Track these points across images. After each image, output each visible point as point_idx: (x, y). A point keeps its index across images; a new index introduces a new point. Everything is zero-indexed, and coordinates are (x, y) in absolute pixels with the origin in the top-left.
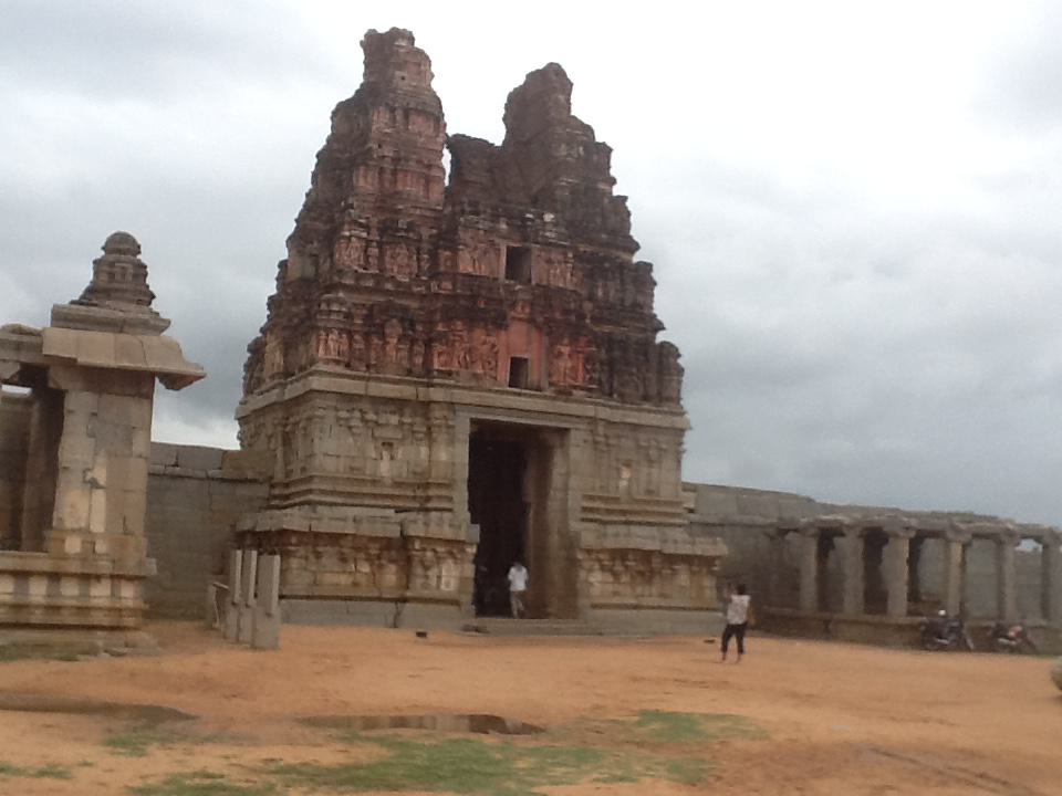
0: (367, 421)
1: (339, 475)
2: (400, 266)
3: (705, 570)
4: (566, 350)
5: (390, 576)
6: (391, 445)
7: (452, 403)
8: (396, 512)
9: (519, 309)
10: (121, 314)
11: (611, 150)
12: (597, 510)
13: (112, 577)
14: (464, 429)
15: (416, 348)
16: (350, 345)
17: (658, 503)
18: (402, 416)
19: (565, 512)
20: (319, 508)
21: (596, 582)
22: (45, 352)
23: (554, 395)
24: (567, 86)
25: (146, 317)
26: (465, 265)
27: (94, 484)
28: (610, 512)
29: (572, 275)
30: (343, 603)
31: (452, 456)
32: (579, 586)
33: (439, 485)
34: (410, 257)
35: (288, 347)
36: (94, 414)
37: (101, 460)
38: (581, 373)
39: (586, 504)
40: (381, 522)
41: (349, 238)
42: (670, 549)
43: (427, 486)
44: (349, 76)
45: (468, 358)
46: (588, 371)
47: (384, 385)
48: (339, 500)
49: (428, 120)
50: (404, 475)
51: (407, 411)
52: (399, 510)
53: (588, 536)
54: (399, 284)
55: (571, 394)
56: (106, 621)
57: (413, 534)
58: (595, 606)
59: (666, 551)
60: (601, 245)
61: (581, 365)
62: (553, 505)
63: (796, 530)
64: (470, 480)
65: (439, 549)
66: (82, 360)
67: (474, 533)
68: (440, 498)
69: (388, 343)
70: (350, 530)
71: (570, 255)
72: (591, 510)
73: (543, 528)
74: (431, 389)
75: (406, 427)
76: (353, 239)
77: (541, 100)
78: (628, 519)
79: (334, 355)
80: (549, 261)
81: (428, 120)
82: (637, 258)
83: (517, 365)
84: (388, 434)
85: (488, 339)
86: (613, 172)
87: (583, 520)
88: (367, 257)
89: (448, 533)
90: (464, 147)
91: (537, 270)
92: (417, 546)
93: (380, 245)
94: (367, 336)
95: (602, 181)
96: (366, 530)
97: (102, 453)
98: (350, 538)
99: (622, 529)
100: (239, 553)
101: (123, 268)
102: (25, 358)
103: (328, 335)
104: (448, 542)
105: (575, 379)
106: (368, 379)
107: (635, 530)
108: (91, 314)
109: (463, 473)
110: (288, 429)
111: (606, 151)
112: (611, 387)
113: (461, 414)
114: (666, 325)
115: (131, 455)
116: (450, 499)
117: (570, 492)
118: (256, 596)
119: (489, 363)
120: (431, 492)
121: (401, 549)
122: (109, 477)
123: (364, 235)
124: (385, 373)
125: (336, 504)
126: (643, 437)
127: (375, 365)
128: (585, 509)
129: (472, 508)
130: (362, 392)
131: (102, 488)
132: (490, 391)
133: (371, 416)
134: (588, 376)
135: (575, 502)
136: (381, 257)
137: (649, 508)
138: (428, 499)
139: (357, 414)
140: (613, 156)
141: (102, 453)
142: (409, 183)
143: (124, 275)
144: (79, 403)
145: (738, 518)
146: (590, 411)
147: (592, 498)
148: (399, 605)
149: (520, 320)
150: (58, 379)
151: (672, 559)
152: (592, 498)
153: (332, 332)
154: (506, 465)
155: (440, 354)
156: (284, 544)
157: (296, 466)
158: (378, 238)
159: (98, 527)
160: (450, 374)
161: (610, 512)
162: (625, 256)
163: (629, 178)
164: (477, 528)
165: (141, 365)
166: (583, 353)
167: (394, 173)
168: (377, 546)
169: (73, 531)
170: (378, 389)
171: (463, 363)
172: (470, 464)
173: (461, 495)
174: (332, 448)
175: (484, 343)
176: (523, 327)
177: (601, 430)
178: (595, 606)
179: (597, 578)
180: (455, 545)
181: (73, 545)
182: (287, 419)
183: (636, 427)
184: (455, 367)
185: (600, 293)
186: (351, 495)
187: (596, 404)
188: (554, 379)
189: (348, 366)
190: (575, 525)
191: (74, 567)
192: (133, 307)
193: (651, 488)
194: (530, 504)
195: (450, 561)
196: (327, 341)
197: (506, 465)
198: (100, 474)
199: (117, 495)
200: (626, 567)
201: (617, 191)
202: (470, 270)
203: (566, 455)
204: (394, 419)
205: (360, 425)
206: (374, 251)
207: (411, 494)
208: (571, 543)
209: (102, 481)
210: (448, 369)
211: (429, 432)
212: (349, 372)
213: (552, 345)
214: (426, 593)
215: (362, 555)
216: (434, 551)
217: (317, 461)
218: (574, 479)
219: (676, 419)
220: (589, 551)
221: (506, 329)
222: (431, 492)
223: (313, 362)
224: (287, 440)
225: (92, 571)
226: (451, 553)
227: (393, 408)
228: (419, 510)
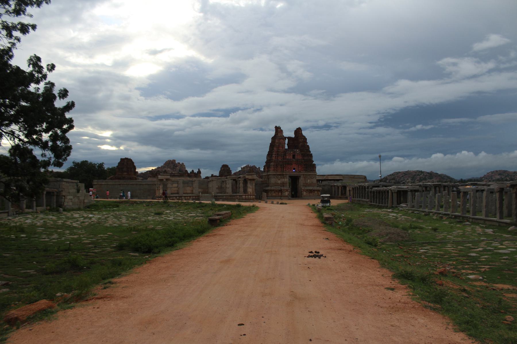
5: (280, 194)
14: (288, 177)
21: (305, 193)
26: (287, 157)
31: (287, 180)
35: (268, 168)
40: (278, 188)
44: (273, 133)
53: (303, 188)
77: (298, 131)
78: (309, 185)
90: (290, 138)
121: (281, 191)
144: (249, 182)
151: (314, 190)
154: (294, 180)
163: (309, 143)
173: (288, 184)
174: (273, 180)
179: (304, 193)
197: (294, 180)
199: (252, 189)
208: (301, 189)
218: (301, 181)
224: (268, 179)
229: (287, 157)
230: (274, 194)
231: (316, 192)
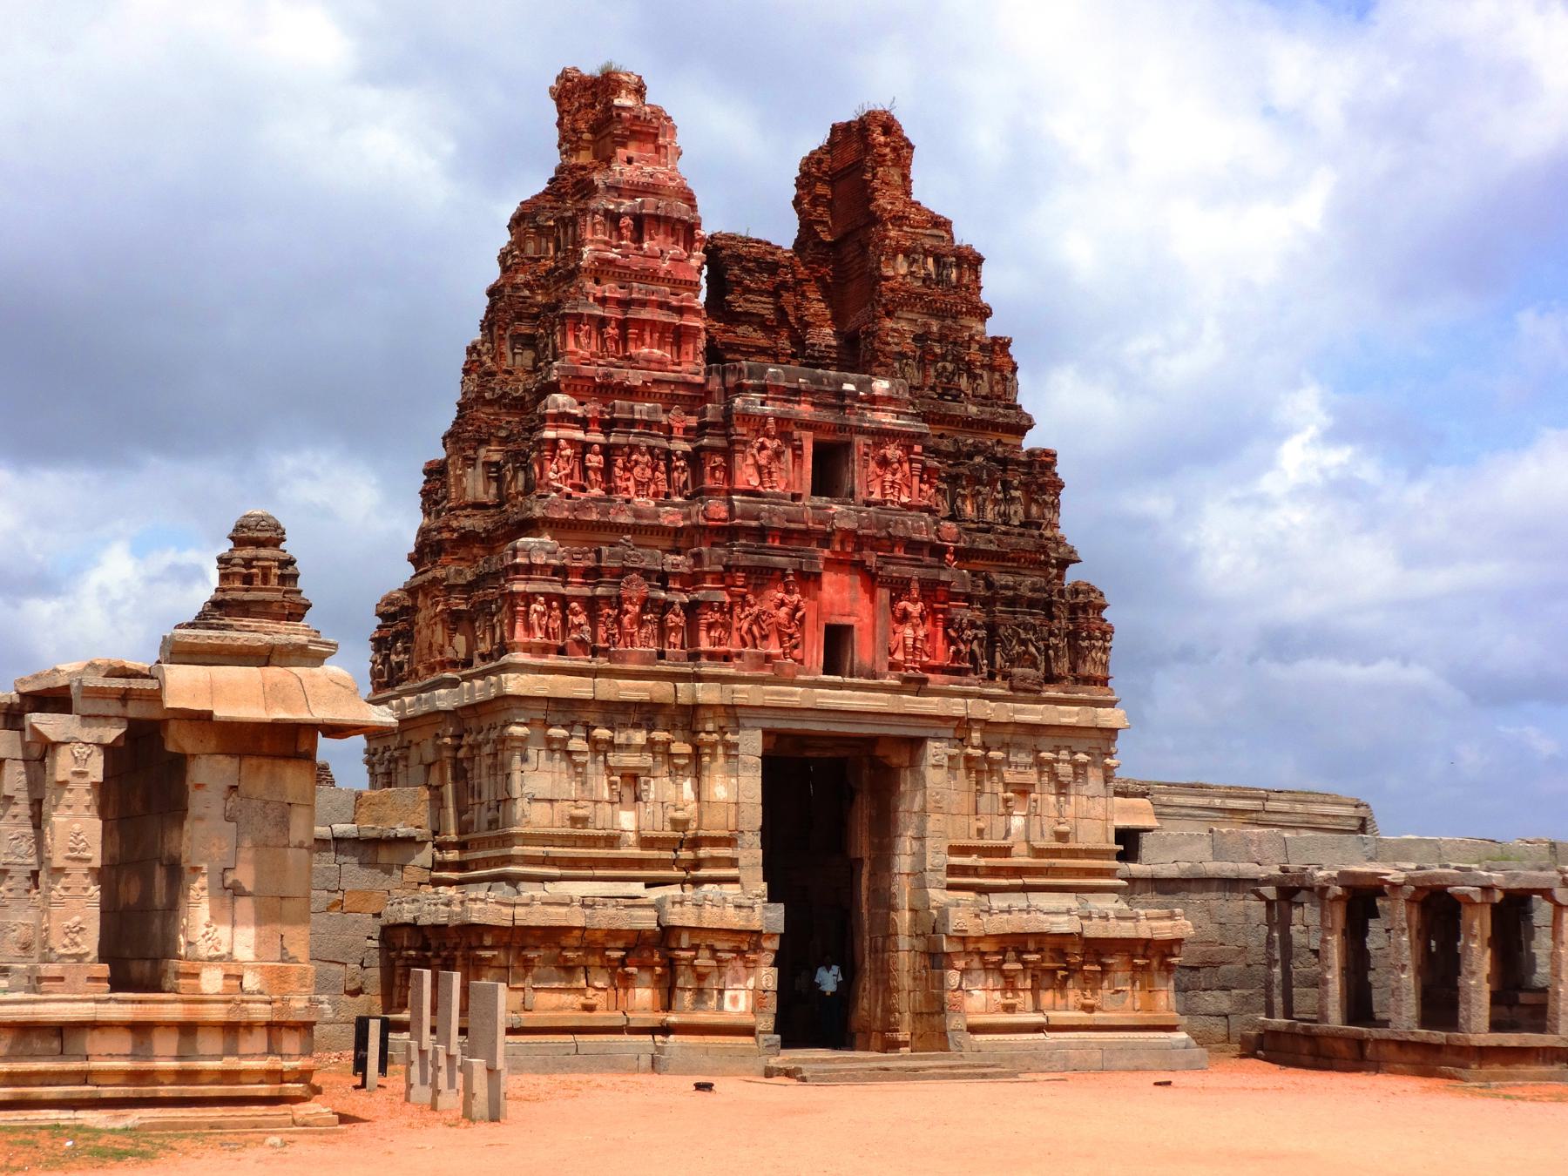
1: (554, 831)
2: (638, 483)
3: (1155, 963)
4: (915, 609)
5: (644, 994)
6: (635, 778)
7: (733, 706)
8: (647, 886)
10: (267, 638)
11: (979, 260)
12: (974, 871)
13: (269, 1025)
14: (751, 743)
15: (672, 619)
16: (565, 620)
17: (1074, 853)
18: (650, 730)
19: (918, 874)
20: (523, 886)
22: (169, 704)
23: (897, 683)
24: (902, 151)
25: (302, 639)
27: (237, 891)
28: (995, 872)
30: (570, 1038)
31: (733, 792)
32: (948, 995)
33: (715, 842)
34: (655, 469)
36: (234, 788)
37: (247, 854)
38: (940, 643)
39: (957, 860)
41: (555, 441)
42: (1094, 930)
43: (696, 843)
45: (755, 629)
46: (951, 641)
48: (556, 872)
50: (658, 825)
51: (660, 720)
52: (651, 884)
54: (638, 514)
55: (925, 680)
56: (264, 1090)
57: (678, 923)
58: (974, 1029)
59: (1088, 934)
60: (970, 424)
61: (940, 629)
62: (903, 863)
63: (1310, 889)
64: (762, 829)
65: (718, 945)
66: (221, 712)
67: (771, 918)
68: (716, 862)
69: (627, 612)
70: (577, 918)
71: (918, 449)
73: (885, 902)
74: (699, 685)
75: (659, 748)
76: (562, 442)
78: (1025, 880)
79: (539, 637)
80: (884, 463)
82: (1030, 441)
83: (837, 639)
84: (630, 760)
85: (787, 598)
86: (986, 297)
87: (951, 887)
88: (585, 470)
89: (735, 920)
91: (866, 480)
92: (685, 942)
93: (608, 451)
94: (591, 605)
96: (605, 918)
97: (247, 843)
98: (577, 933)
99: (1018, 900)
100: (427, 973)
101: (263, 568)
102: (134, 710)
103: (528, 606)
106: (595, 673)
107: (1038, 899)
108: (228, 642)
109: (754, 816)
110: (461, 754)
111: (971, 261)
112: (992, 663)
114: (1080, 555)
115: (287, 846)
116: (733, 863)
117: (929, 843)
118: (433, 1030)
119: (791, 636)
120: (704, 852)
122: (257, 881)
123: (579, 435)
124: (623, 661)
125: (552, 879)
127: (606, 649)
128: (953, 870)
129: (771, 872)
130: (590, 696)
131: (249, 895)
132: (793, 683)
133: (602, 733)
134: (953, 648)
135: (938, 858)
136: (607, 471)
138: (697, 864)
139: (580, 732)
140: (985, 270)
141: (247, 843)
142: (648, 340)
143: (265, 579)
144: (210, 775)
145: (1212, 867)
148: (658, 1038)
150: (178, 740)
151: (1098, 949)
153: (535, 601)
154: (827, 805)
155: (710, 627)
156: (471, 948)
157: (481, 816)
158: (601, 438)
159: (245, 953)
160: (727, 657)
161: (995, 872)
162: (1008, 439)
164: (778, 911)
165: (303, 715)
167: (623, 325)
168: (620, 944)
169: (211, 959)
170: (608, 689)
171: (748, 638)
172: (766, 803)
173: (751, 853)
175: (782, 603)
177: (976, 737)
178: (974, 1029)
180: (745, 942)
181: (212, 981)
182: (461, 737)
184: (733, 646)
185: (969, 509)
186: (574, 863)
187: (966, 695)
188: (899, 656)
189: (561, 651)
190: (938, 896)
191: (217, 1013)
192: (283, 626)
193: (1063, 828)
194: (861, 860)
195: (739, 964)
196: (527, 613)
197: (827, 805)
198: (245, 875)
200: (1024, 963)
201: (992, 328)
202: (755, 482)
203: (920, 782)
204: (639, 737)
205: (584, 746)
206: (595, 460)
207: (668, 855)
209: (249, 887)
210: (723, 648)
211: (696, 755)
212: (564, 662)
213: (893, 601)
214: (701, 1017)
215: (595, 960)
216: (714, 950)
217: (521, 806)
220: (963, 940)
222: (704, 852)
223: (504, 649)
225: (243, 1018)
226: (740, 952)
227: (636, 718)
228: (683, 882)
230: (554, 1003)
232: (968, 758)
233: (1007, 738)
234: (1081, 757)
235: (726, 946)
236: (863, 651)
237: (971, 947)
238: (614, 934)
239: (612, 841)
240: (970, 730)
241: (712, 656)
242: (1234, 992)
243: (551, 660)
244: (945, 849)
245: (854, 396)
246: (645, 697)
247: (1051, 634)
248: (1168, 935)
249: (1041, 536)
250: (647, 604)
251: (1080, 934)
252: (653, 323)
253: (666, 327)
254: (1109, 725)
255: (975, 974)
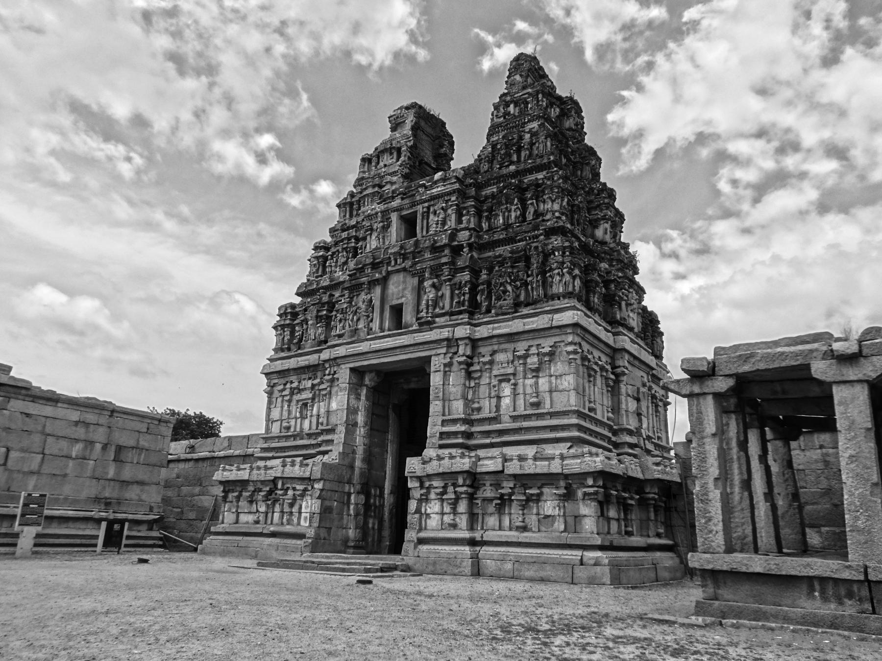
0: (295, 389)
7: (335, 359)
9: (393, 263)
28: (487, 434)
29: (459, 216)
34: (348, 258)
47: (299, 359)
48: (270, 455)
49: (391, 154)
55: (434, 322)
70: (246, 477)
72: (455, 434)
81: (391, 154)
87: (441, 447)
95: (529, 121)
104: (302, 479)
105: (443, 308)
113: (343, 366)
119: (368, 316)
125: (270, 458)
126: (521, 347)
132: (367, 340)
133: (295, 385)
137: (526, 424)
146: (445, 333)
147: (454, 421)
149: (398, 271)
152: (454, 421)
166: (450, 280)
176: (401, 276)
183: (512, 337)
189: (289, 349)
204: (309, 384)
219: (556, 316)
221: (379, 284)
229: (373, 243)
231: (549, 507)
232: (460, 363)
233: (496, 347)
234: (547, 350)
235: (300, 487)
236: (408, 316)
237: (427, 484)
238: (263, 482)
239: (294, 437)
240: (458, 346)
241: (340, 336)
242: (824, 529)
243: (283, 355)
244: (440, 423)
245: (423, 185)
246: (307, 363)
247: (528, 276)
248: (577, 470)
249: (543, 220)
250: (318, 318)
251: (502, 471)
252: (367, 195)
253: (373, 194)
254: (560, 323)
255: (433, 503)
